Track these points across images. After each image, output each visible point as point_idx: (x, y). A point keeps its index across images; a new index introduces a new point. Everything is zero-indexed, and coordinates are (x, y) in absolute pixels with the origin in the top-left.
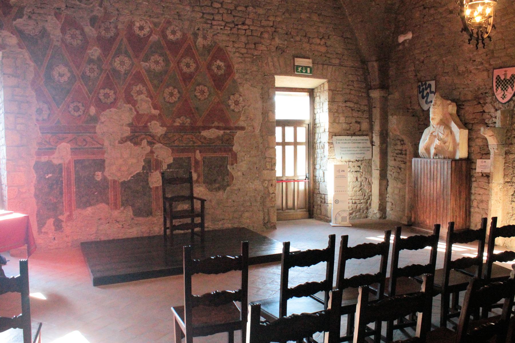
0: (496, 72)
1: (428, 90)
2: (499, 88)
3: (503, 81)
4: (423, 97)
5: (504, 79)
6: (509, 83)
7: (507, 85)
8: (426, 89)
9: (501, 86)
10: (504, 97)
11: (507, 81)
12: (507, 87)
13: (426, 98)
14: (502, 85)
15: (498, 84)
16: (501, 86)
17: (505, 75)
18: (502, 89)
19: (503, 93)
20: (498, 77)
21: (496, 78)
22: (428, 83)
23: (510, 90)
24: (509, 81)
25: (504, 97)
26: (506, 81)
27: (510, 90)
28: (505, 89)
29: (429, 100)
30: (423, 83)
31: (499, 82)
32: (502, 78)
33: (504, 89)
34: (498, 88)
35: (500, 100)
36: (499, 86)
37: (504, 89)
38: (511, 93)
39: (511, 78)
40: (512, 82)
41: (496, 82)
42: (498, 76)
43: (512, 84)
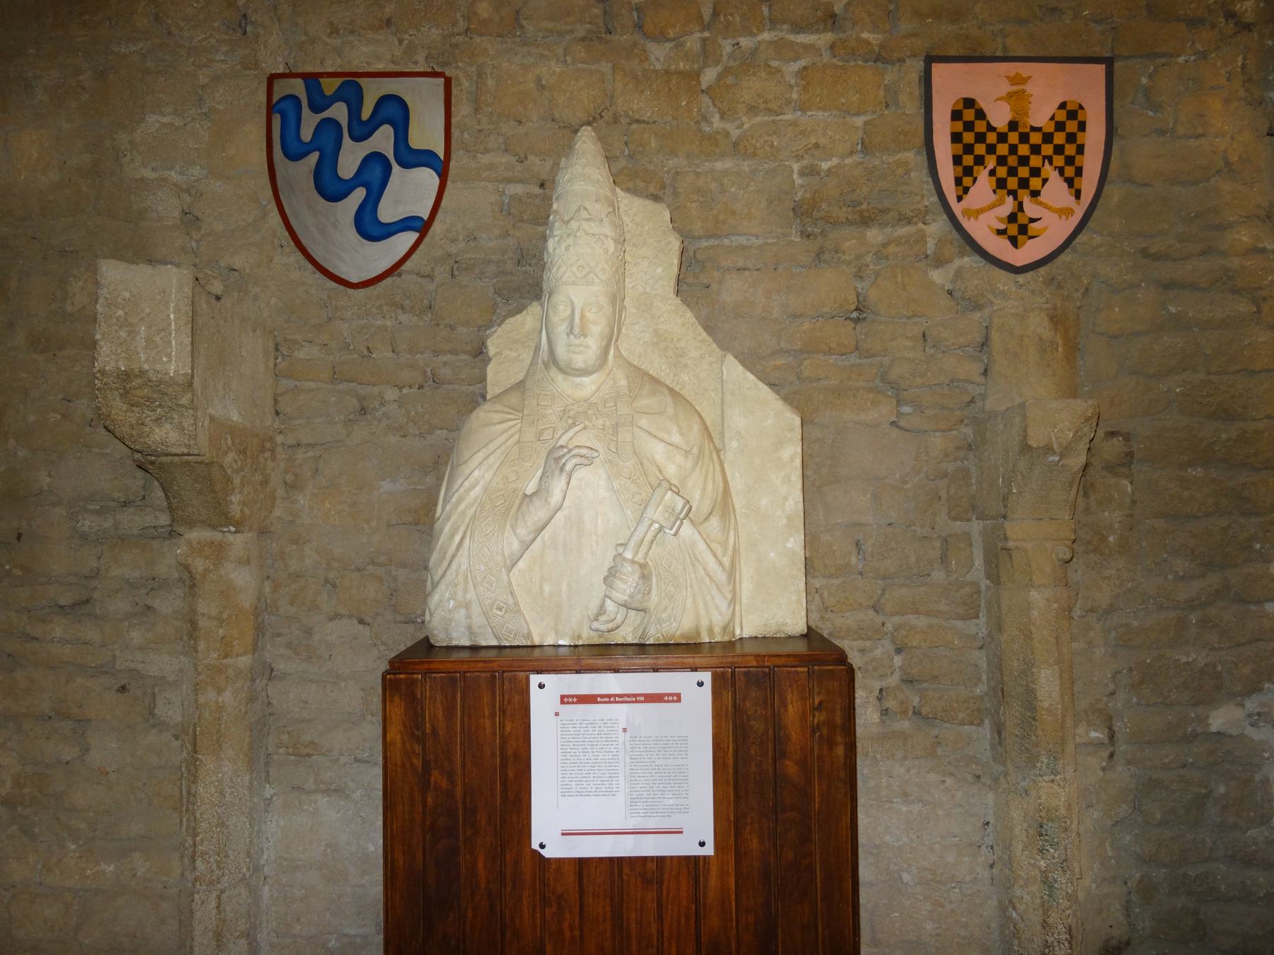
0: (952, 82)
1: (383, 140)
2: (983, 175)
3: (1002, 138)
4: (330, 188)
5: (1013, 125)
6: (1047, 149)
7: (1035, 161)
8: (361, 131)
9: (991, 162)
10: (1017, 229)
11: (1035, 138)
12: (1036, 172)
13: (359, 194)
14: (1002, 161)
15: (969, 149)
16: (991, 162)
17: (1017, 98)
18: (1001, 184)
19: (1009, 205)
20: (968, 113)
21: (956, 115)
22: (373, 91)
23: (1055, 189)
24: (1048, 138)
25: (1017, 229)
26: (1024, 138)
27: (1055, 189)
28: (1024, 183)
29: (388, 212)
30: (329, 86)
31: (980, 138)
32: (999, 117)
33: (1012, 183)
34: (968, 171)
35: (1000, 248)
36: (980, 161)
37: (1012, 183)
38: (1068, 212)
39: (1060, 126)
40: (1070, 150)
41: (956, 138)
42: (969, 103)
43: (1070, 161)
